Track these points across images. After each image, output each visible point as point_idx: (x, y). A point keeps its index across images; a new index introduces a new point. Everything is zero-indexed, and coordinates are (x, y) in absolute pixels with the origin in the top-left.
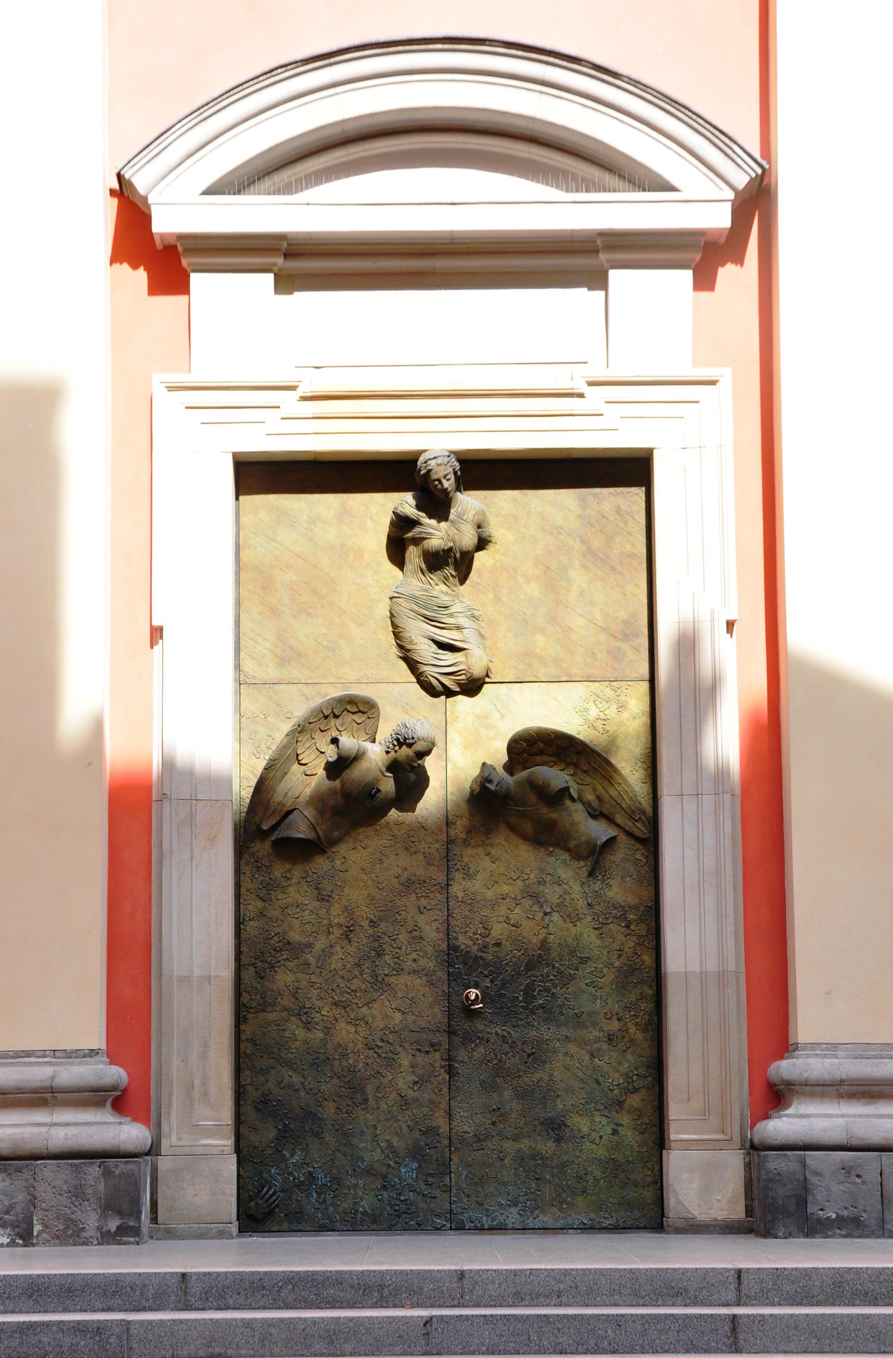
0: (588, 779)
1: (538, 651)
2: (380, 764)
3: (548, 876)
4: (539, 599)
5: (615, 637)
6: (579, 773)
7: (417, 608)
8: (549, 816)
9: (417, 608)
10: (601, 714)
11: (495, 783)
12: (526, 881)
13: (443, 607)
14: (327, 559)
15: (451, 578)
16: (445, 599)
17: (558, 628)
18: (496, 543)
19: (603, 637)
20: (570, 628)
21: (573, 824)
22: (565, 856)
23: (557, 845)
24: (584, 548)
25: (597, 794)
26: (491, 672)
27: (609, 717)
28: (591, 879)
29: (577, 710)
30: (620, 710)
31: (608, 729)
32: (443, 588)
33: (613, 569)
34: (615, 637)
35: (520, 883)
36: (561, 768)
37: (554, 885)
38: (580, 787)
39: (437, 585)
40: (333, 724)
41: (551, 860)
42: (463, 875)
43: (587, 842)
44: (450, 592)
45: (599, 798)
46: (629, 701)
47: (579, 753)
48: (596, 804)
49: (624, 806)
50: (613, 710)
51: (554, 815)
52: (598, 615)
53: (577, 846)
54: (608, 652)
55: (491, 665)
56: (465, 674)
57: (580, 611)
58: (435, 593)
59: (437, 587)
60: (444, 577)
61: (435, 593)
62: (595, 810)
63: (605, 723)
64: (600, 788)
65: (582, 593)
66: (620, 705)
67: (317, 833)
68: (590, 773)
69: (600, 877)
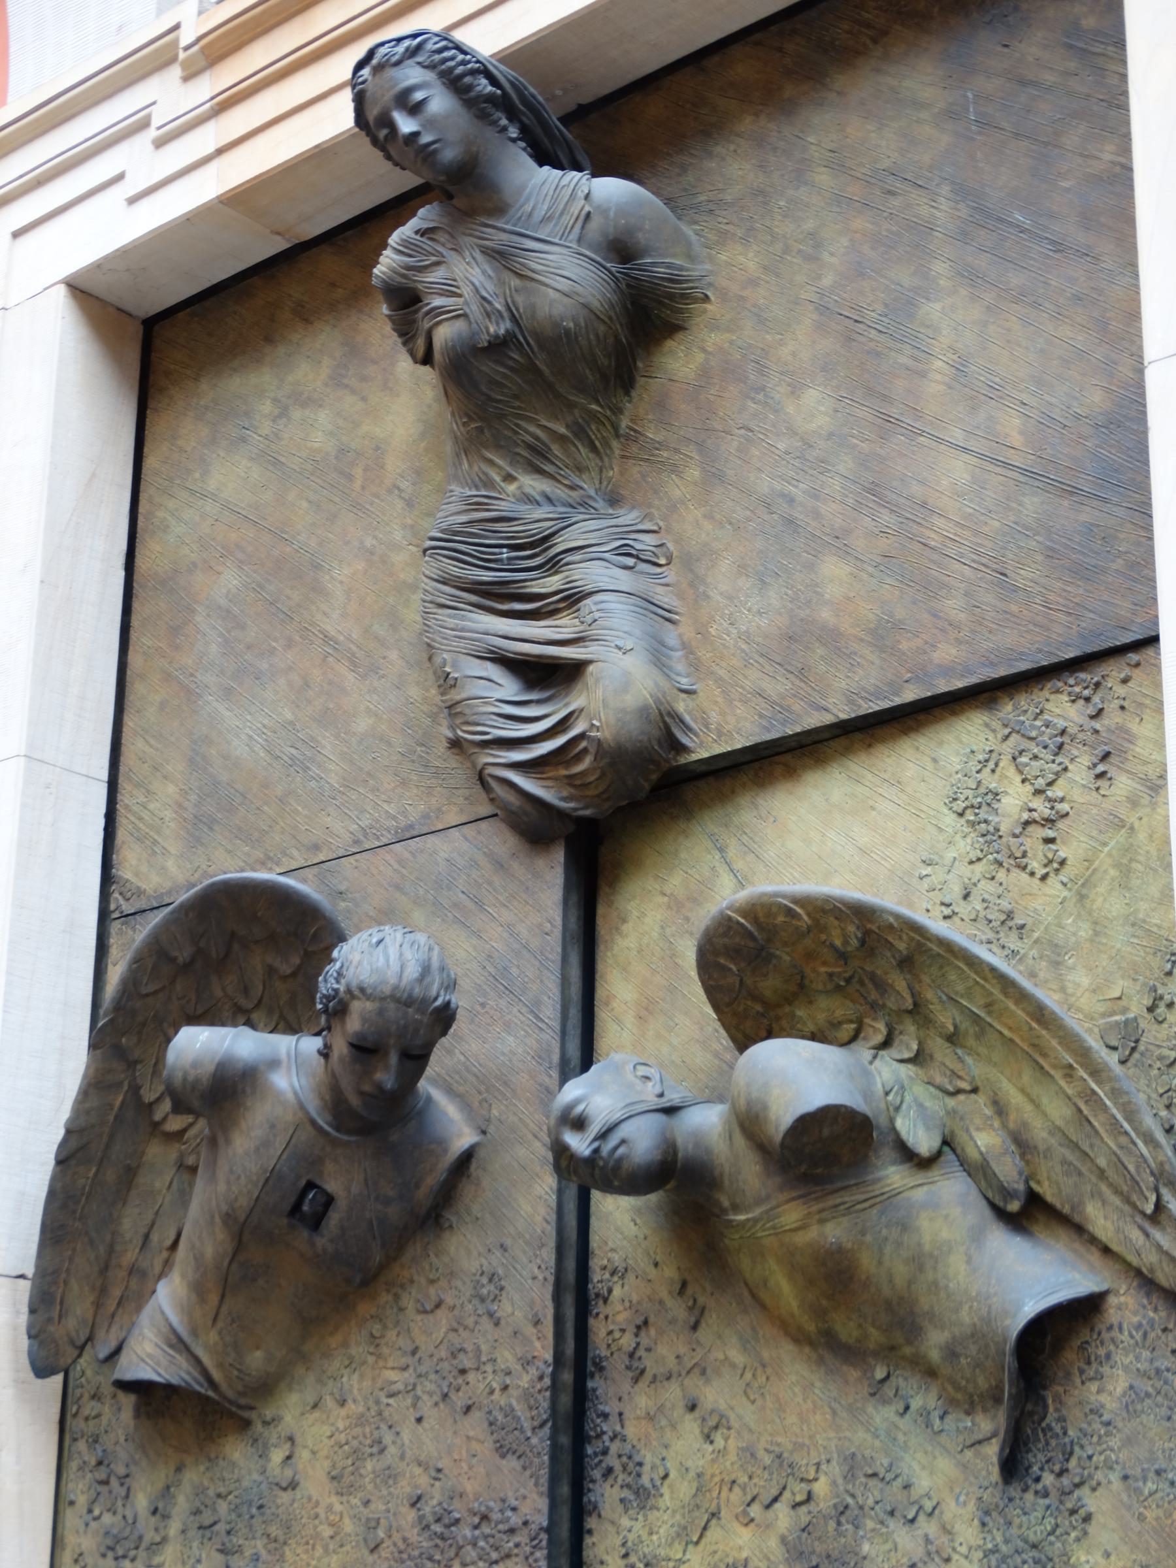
0: (975, 1068)
1: (826, 615)
2: (313, 1106)
3: (872, 1483)
4: (830, 435)
5: (1073, 492)
6: (938, 1047)
7: (455, 569)
8: (812, 1233)
9: (455, 569)
10: (1037, 803)
11: (594, 1129)
12: (804, 1509)
13: (532, 545)
14: (305, 504)
15: (556, 449)
16: (538, 518)
17: (886, 517)
18: (706, 299)
19: (1032, 504)
20: (924, 505)
21: (919, 1261)
22: (924, 1398)
23: (888, 1352)
24: (964, 212)
25: (1011, 1125)
26: (687, 728)
27: (1064, 807)
28: (1014, 1491)
29: (960, 805)
30: (1101, 768)
31: (1062, 854)
32: (532, 484)
33: (1059, 247)
34: (1073, 492)
35: (783, 1518)
36: (879, 1038)
37: (892, 1524)
38: (951, 1102)
39: (509, 478)
40: (218, 993)
41: (883, 1415)
42: (625, 1493)
43: (975, 1335)
44: (559, 492)
45: (1022, 1144)
46: (1134, 727)
47: (906, 963)
48: (1008, 1170)
49: (1102, 1162)
50: (1080, 770)
51: (834, 1232)
52: (1012, 426)
53: (951, 1353)
54: (1051, 554)
55: (682, 706)
56: (585, 750)
57: (957, 435)
58: (505, 507)
59: (512, 488)
60: (530, 447)
61: (503, 505)
62: (1008, 1194)
63: (1051, 834)
64: (1014, 1097)
65: (960, 369)
66: (1100, 751)
67: (197, 1361)
68: (971, 1042)
69: (1048, 1479)
